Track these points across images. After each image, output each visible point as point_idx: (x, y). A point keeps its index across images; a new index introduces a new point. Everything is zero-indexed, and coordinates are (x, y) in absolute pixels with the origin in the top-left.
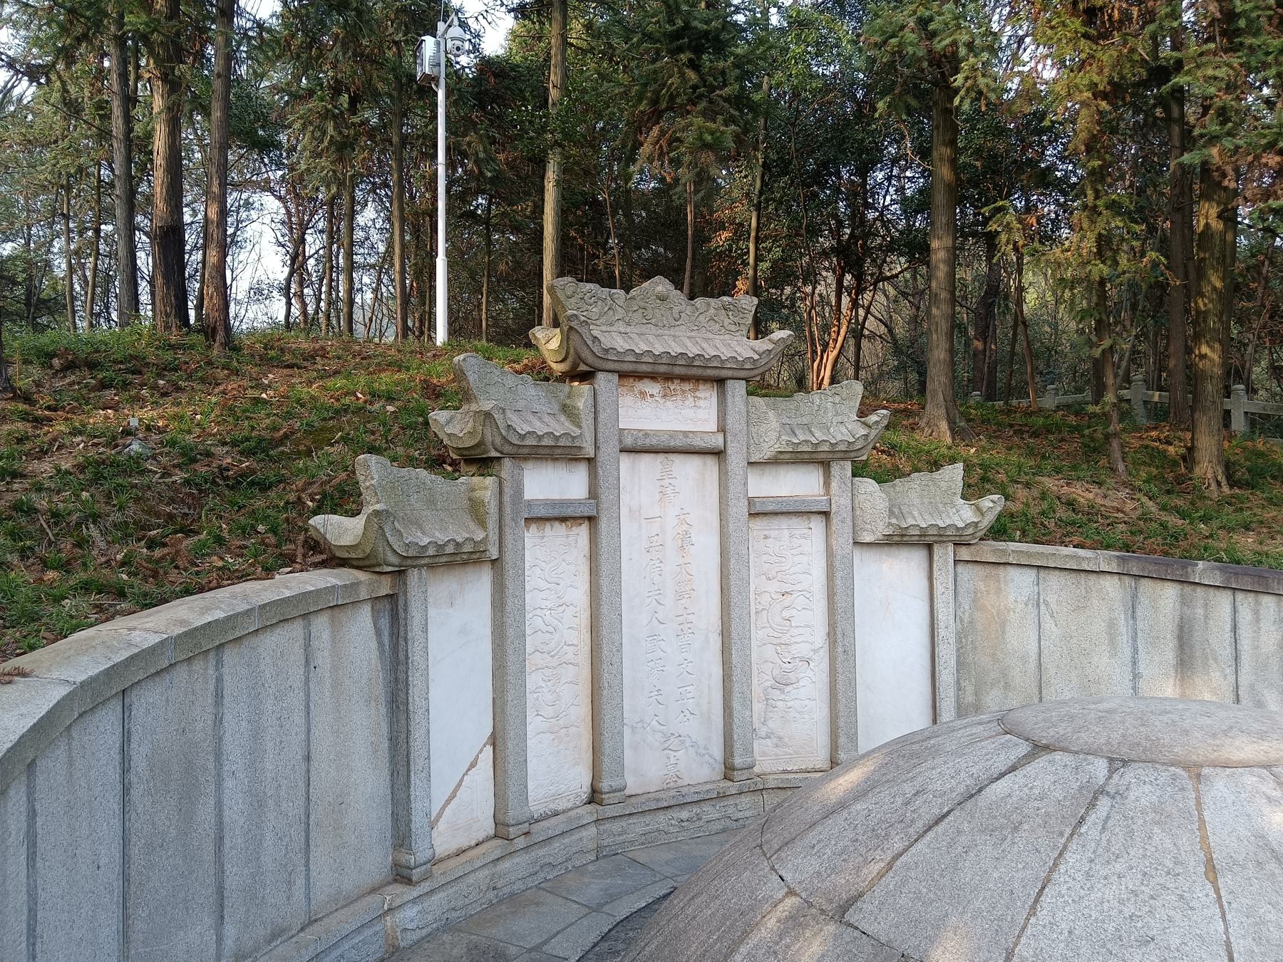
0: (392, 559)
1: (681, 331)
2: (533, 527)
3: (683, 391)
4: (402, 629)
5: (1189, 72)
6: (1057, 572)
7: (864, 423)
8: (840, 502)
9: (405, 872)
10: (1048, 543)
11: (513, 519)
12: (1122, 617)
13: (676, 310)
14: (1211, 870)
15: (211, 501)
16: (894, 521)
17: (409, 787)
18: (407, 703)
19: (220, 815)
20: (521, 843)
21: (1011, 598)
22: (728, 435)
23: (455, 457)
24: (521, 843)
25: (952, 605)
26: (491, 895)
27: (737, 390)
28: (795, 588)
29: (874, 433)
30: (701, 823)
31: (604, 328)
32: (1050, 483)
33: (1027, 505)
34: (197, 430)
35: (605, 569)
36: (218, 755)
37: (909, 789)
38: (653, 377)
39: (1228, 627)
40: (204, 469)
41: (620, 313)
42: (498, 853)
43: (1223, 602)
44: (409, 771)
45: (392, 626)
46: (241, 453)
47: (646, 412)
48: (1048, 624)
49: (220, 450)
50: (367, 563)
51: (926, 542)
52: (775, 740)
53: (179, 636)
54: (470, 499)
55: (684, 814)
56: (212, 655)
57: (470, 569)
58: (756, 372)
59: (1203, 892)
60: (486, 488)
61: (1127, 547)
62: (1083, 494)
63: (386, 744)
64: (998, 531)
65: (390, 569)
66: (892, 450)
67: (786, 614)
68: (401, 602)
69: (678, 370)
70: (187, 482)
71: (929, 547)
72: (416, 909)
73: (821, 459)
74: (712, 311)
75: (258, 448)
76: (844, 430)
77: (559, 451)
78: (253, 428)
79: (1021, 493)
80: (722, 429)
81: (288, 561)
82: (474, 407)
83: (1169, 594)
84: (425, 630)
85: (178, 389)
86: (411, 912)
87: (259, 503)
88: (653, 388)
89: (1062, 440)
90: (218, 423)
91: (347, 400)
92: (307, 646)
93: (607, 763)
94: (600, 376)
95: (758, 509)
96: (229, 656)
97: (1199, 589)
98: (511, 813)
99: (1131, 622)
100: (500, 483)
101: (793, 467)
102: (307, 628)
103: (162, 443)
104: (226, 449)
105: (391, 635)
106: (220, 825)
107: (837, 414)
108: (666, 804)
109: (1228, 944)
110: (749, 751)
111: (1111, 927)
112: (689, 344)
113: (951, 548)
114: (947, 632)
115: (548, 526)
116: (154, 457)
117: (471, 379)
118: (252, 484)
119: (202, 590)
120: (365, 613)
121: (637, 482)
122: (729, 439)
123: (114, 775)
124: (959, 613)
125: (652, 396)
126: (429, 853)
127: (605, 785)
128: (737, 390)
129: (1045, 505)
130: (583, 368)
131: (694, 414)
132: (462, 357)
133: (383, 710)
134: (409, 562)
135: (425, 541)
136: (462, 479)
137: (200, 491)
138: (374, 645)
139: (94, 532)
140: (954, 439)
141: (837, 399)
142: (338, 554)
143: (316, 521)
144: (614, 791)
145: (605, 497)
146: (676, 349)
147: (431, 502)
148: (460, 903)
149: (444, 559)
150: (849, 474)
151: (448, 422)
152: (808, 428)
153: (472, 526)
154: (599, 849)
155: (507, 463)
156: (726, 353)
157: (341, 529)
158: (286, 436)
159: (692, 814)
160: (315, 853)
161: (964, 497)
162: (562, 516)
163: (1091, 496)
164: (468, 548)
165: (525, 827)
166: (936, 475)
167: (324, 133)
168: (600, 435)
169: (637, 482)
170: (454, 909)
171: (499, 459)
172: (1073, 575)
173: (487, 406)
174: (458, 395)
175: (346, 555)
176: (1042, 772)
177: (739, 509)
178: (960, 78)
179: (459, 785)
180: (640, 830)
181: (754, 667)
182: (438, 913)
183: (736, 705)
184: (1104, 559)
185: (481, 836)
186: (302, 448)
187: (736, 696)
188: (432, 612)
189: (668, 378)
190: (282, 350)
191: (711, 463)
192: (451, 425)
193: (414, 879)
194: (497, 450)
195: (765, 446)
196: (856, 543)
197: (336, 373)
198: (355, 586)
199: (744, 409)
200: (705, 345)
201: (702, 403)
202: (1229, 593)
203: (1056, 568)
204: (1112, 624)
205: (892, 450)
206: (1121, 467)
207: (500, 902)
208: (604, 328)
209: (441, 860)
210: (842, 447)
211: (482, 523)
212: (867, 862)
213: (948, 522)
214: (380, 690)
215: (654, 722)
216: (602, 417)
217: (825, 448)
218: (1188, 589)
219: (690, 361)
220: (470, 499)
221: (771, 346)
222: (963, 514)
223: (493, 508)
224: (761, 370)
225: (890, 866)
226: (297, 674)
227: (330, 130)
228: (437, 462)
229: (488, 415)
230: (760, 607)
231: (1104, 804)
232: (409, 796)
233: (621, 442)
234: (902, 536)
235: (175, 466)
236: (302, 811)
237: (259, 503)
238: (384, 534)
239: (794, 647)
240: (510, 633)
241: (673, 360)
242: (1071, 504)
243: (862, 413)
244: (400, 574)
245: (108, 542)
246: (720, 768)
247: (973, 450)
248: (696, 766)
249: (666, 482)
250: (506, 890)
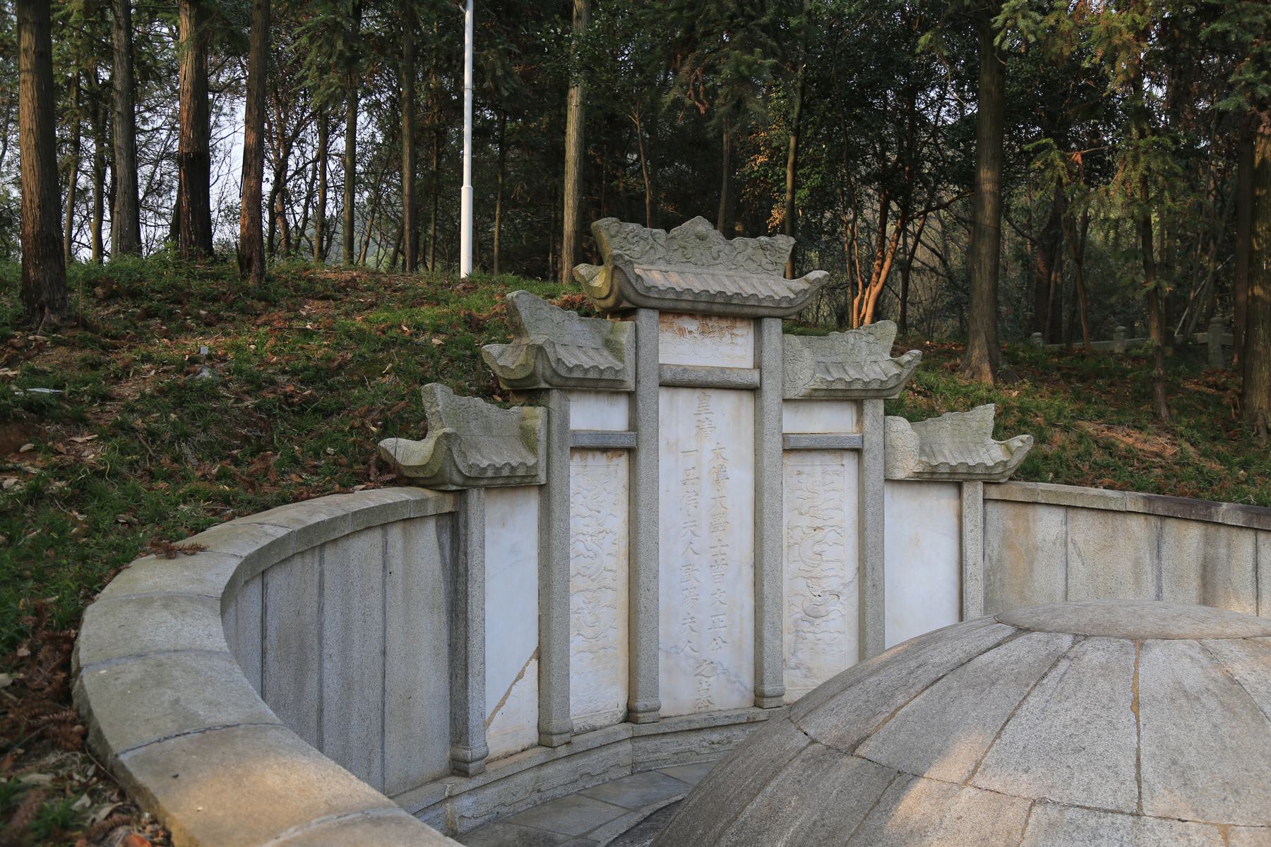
0: (457, 478)
1: (720, 271)
2: (577, 457)
3: (721, 329)
4: (462, 544)
5: (1228, 18)
6: (1085, 512)
7: (897, 363)
8: (873, 439)
9: (463, 765)
10: (1079, 484)
11: (560, 448)
12: (1148, 556)
13: (715, 249)
14: (1136, 705)
15: (281, 426)
16: (924, 459)
17: (467, 689)
18: (466, 611)
19: (321, 690)
20: (563, 751)
21: (1040, 537)
22: (764, 372)
23: (505, 388)
24: (563, 751)
25: (980, 543)
26: (536, 796)
27: (773, 328)
28: (828, 523)
29: (906, 372)
30: (731, 746)
31: (645, 267)
32: (1090, 428)
33: (1063, 448)
34: (256, 360)
35: (643, 498)
36: (320, 638)
37: (913, 664)
38: (692, 314)
39: (1250, 567)
40: (271, 396)
41: (661, 252)
42: (542, 759)
43: (1245, 542)
44: (467, 675)
45: (452, 541)
46: (302, 382)
47: (686, 348)
48: (1075, 563)
49: (282, 379)
50: (433, 482)
51: (955, 480)
52: (804, 671)
53: (299, 531)
54: (521, 428)
55: (715, 737)
56: (317, 551)
57: (520, 493)
58: (793, 311)
59: (1127, 719)
60: (536, 417)
61: (1159, 490)
62: (1125, 438)
63: (446, 650)
64: (1029, 471)
65: (454, 488)
66: (928, 391)
67: (817, 548)
68: (462, 519)
69: (716, 308)
70: (258, 408)
71: (959, 486)
72: (472, 799)
73: (854, 397)
74: (750, 250)
75: (318, 376)
76: (878, 369)
77: (603, 384)
78: (308, 358)
79: (1059, 437)
80: (758, 366)
81: (362, 478)
82: (525, 341)
83: (1192, 535)
84: (482, 546)
85: (220, 319)
86: (466, 802)
87: (325, 428)
88: (691, 325)
89: (1112, 385)
90: (274, 354)
91: (393, 333)
92: (385, 553)
93: (642, 684)
94: (643, 314)
95: (792, 444)
96: (329, 553)
97: (1223, 530)
98: (554, 722)
99: (1156, 561)
100: (549, 414)
101: (827, 404)
102: (385, 535)
103: (229, 370)
104: (286, 378)
105: (452, 549)
106: (321, 697)
107: (871, 354)
108: (698, 726)
109: (1138, 750)
110: (778, 679)
111: (1054, 743)
112: (728, 283)
113: (980, 486)
114: (975, 567)
115: (590, 455)
116: (225, 385)
117: (523, 314)
118: (315, 410)
119: (296, 500)
120: (431, 526)
121: (675, 416)
122: (765, 376)
123: (258, 640)
124: (988, 551)
126: (483, 750)
127: (641, 704)
128: (773, 328)
129: (1082, 449)
130: (625, 304)
131: (730, 350)
132: (515, 294)
133: (444, 618)
134: (471, 482)
135: (485, 463)
136: (514, 409)
137: (269, 416)
138: (437, 557)
139: (187, 451)
140: (995, 381)
141: (871, 338)
142: (407, 474)
143: (387, 443)
144: (649, 711)
145: (645, 429)
146: (714, 288)
147: (488, 429)
148: (509, 800)
149: (500, 482)
150: (882, 412)
151: (500, 355)
152: (841, 366)
153: (524, 452)
154: (634, 764)
155: (555, 395)
156: (763, 292)
157: (410, 452)
158: (340, 367)
159: (723, 737)
160: (389, 738)
161: (995, 435)
162: (603, 447)
163: (1131, 441)
164: (521, 472)
165: (566, 737)
166: (967, 415)
167: (333, 46)
168: (641, 369)
169: (675, 416)
170: (503, 804)
171: (547, 390)
172: (1101, 515)
173: (540, 340)
174: (510, 327)
175: (414, 475)
176: (1022, 648)
177: (773, 445)
178: (1000, 18)
179: (508, 693)
180: (673, 748)
181: (785, 599)
182: (490, 806)
183: (767, 634)
184: (1131, 500)
185: (526, 743)
186: (356, 378)
187: (767, 626)
188: (488, 531)
189: (706, 315)
190: (310, 280)
191: (747, 400)
192: (502, 357)
193: (471, 771)
194: (546, 382)
195: (800, 383)
196: (887, 480)
197: (371, 305)
198: (422, 503)
199: (779, 347)
200: (742, 284)
201: (739, 340)
202: (1252, 533)
203: (1083, 508)
204: (1137, 563)
205: (928, 391)
206: (1164, 412)
207: (544, 803)
208: (645, 267)
209: (491, 761)
210: (875, 386)
211: (532, 449)
212: (875, 714)
213: (978, 460)
214: (441, 598)
215: (688, 648)
216: (642, 352)
217: (858, 386)
218: (1212, 529)
219: (728, 300)
220: (521, 428)
221: (806, 286)
222: (993, 454)
223: (542, 436)
224: (797, 309)
225: (893, 715)
226: (377, 576)
227: (340, 45)
228: (488, 393)
229: (540, 349)
230: (792, 541)
231: (1064, 665)
232: (467, 696)
233: (660, 376)
234: (933, 473)
235: (247, 392)
236: (379, 699)
237: (325, 428)
238: (451, 456)
240: (556, 554)
241: (712, 298)
242: (1109, 448)
243: (896, 352)
244: (461, 494)
245: (199, 460)
246: (750, 696)
247: (1015, 394)
248: (729, 695)
249: (702, 417)
250: (549, 794)
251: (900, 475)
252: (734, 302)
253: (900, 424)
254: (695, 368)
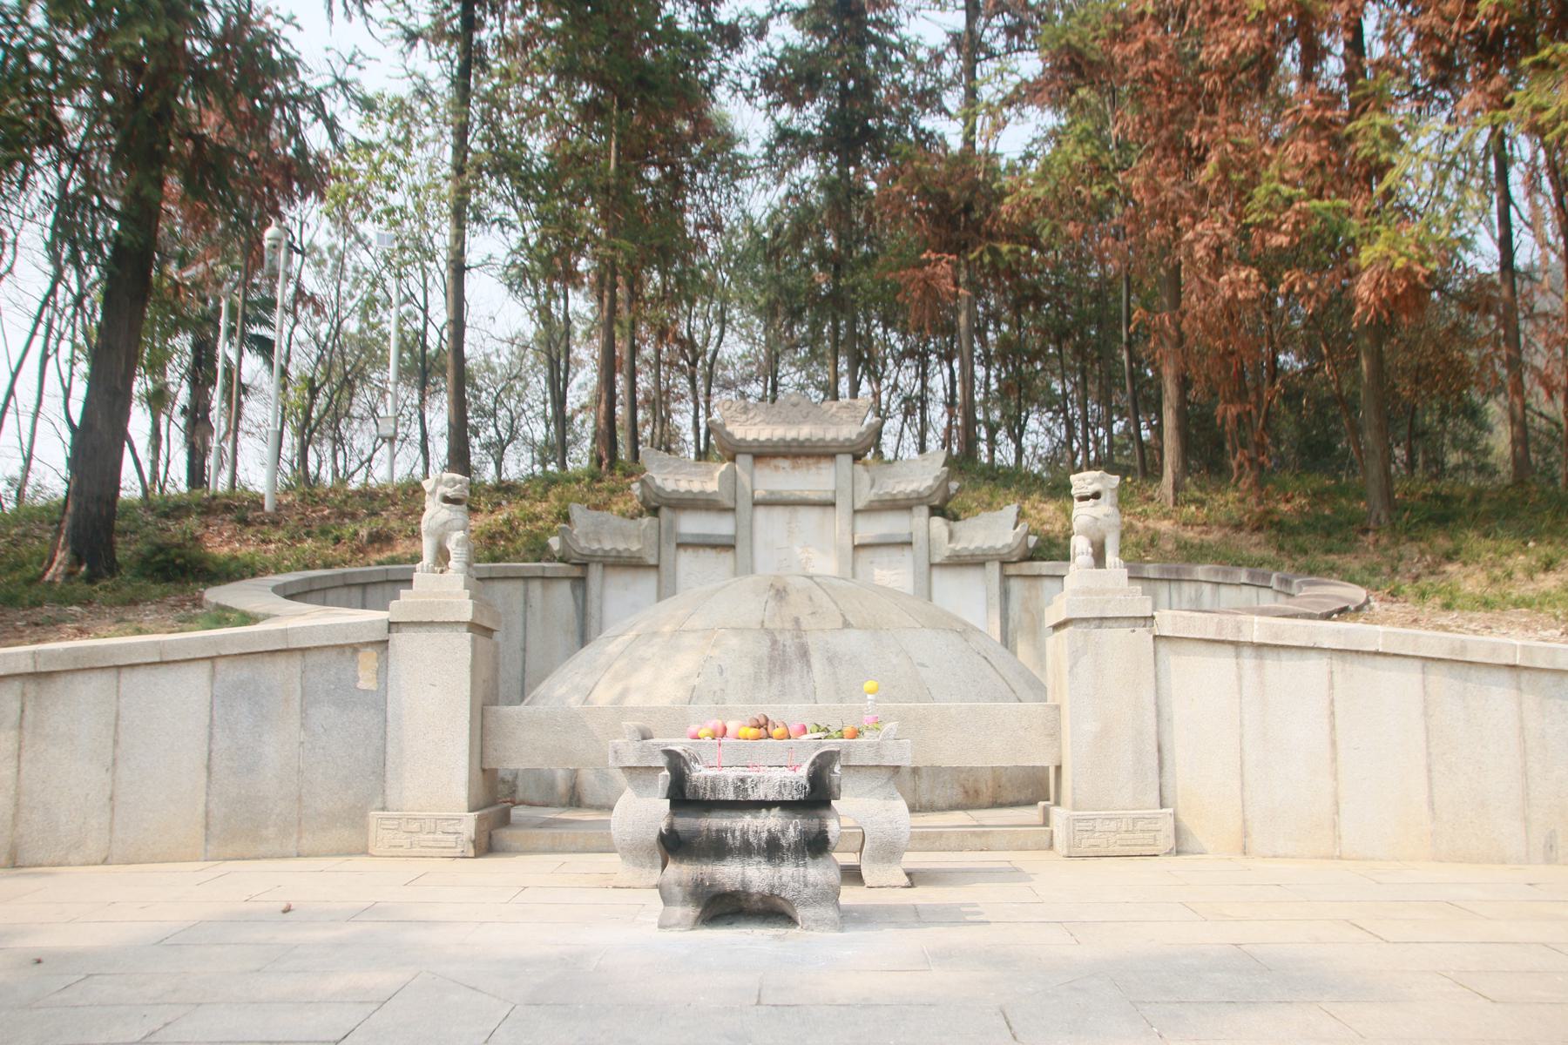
27: (845, 461)
38: (785, 456)
88: (785, 463)
94: (739, 458)
115: (701, 551)
169: (769, 524)
189: (796, 456)
199: (849, 474)
201: (824, 472)
244: (586, 565)
251: (937, 559)
253: (938, 522)
254: (780, 492)
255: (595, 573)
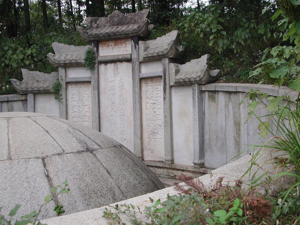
67: (155, 110)
88: (111, 43)
125: (111, 45)
131: (125, 49)
166: (198, 60)
201: (128, 45)
239: (157, 121)
252: (117, 34)
253: (172, 65)
255: (30, 97)
